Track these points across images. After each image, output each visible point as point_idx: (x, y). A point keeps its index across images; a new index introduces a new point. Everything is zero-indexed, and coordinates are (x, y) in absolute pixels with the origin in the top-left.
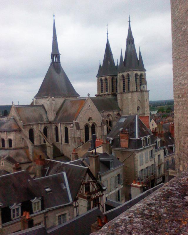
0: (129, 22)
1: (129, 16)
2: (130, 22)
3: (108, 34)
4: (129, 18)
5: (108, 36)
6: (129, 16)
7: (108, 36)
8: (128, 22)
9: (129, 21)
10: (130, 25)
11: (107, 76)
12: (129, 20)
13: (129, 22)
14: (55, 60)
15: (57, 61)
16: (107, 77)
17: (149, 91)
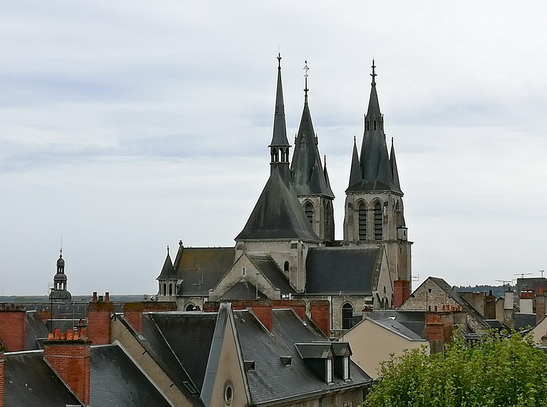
0: (374, 75)
1: (373, 63)
2: (375, 77)
3: (306, 90)
4: (373, 67)
5: (306, 96)
6: (373, 63)
7: (306, 96)
8: (372, 77)
9: (372, 74)
10: (374, 84)
11: (314, 196)
12: (373, 72)
13: (374, 75)
14: (285, 161)
15: (280, 161)
16: (312, 199)
17: (412, 243)
